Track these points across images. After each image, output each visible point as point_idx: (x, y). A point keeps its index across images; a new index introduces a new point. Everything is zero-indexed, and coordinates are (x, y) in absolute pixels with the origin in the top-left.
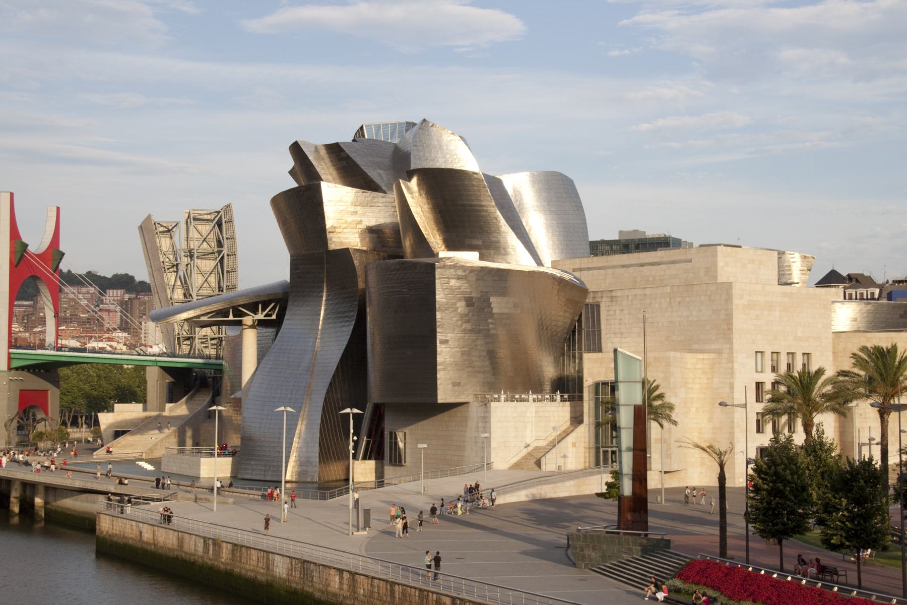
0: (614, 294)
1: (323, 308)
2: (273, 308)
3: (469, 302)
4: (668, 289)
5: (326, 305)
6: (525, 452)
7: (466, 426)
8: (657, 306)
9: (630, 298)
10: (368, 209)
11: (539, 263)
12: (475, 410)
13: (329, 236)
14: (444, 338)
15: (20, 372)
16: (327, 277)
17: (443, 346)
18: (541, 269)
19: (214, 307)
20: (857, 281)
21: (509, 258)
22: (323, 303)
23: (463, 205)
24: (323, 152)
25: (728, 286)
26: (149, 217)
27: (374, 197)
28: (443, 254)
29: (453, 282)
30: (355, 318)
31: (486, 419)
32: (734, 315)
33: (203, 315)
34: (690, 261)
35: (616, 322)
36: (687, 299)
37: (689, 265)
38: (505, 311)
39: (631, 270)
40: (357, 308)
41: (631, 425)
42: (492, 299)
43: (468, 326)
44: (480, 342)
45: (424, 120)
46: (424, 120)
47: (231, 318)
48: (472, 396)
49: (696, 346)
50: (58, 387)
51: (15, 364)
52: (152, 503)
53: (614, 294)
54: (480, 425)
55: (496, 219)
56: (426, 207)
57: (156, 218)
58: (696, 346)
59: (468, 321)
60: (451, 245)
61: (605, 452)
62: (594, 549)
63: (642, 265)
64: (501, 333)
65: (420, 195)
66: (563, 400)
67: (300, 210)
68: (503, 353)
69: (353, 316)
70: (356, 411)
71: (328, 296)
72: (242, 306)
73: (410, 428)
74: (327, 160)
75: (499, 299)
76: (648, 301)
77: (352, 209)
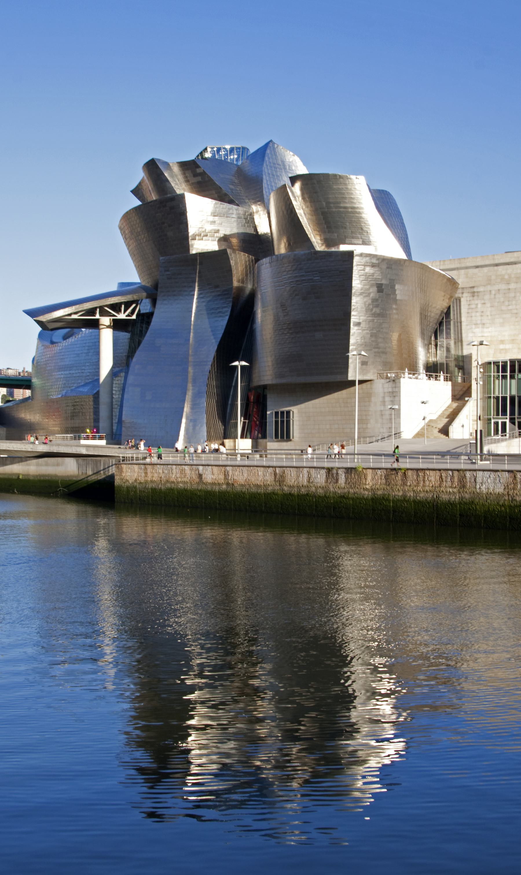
0: (475, 290)
5: (198, 302)
6: (422, 424)
7: (370, 401)
9: (493, 292)
10: (223, 219)
12: (380, 387)
13: (191, 242)
14: (357, 321)
16: (199, 277)
17: (356, 328)
23: (345, 208)
24: (176, 169)
27: (229, 209)
29: (368, 269)
30: (228, 313)
31: (395, 395)
33: (76, 313)
35: (478, 314)
39: (485, 270)
40: (231, 304)
42: (397, 287)
45: (271, 141)
48: (376, 375)
53: (475, 290)
54: (387, 399)
61: (496, 424)
63: (497, 265)
65: (303, 198)
66: (446, 379)
67: (157, 221)
69: (227, 311)
71: (199, 295)
73: (299, 406)
76: (512, 295)
77: (211, 218)
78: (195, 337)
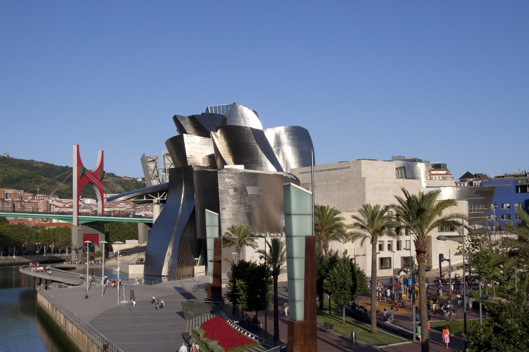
1: (183, 194)
2: (165, 195)
3: (236, 190)
4: (338, 182)
5: (184, 192)
8: (333, 189)
10: (207, 146)
11: (282, 170)
13: (188, 159)
15: (84, 226)
18: (280, 173)
19: (136, 194)
20: (479, 177)
21: (263, 168)
22: (183, 191)
24: (188, 120)
25: (363, 181)
26: (144, 154)
28: (231, 165)
29: (227, 180)
32: (366, 194)
34: (350, 167)
36: (346, 186)
37: (349, 170)
38: (255, 193)
39: (324, 172)
41: (213, 248)
43: (235, 201)
44: (242, 209)
45: (234, 103)
46: (234, 103)
47: (145, 199)
49: (350, 209)
50: (104, 233)
51: (81, 222)
52: (70, 287)
55: (256, 149)
56: (225, 144)
57: (146, 155)
58: (350, 209)
59: (235, 199)
60: (236, 162)
62: (192, 310)
63: (329, 170)
64: (253, 204)
68: (256, 214)
70: (89, 242)
72: (150, 194)
74: (190, 124)
75: (251, 188)
78: (182, 210)
